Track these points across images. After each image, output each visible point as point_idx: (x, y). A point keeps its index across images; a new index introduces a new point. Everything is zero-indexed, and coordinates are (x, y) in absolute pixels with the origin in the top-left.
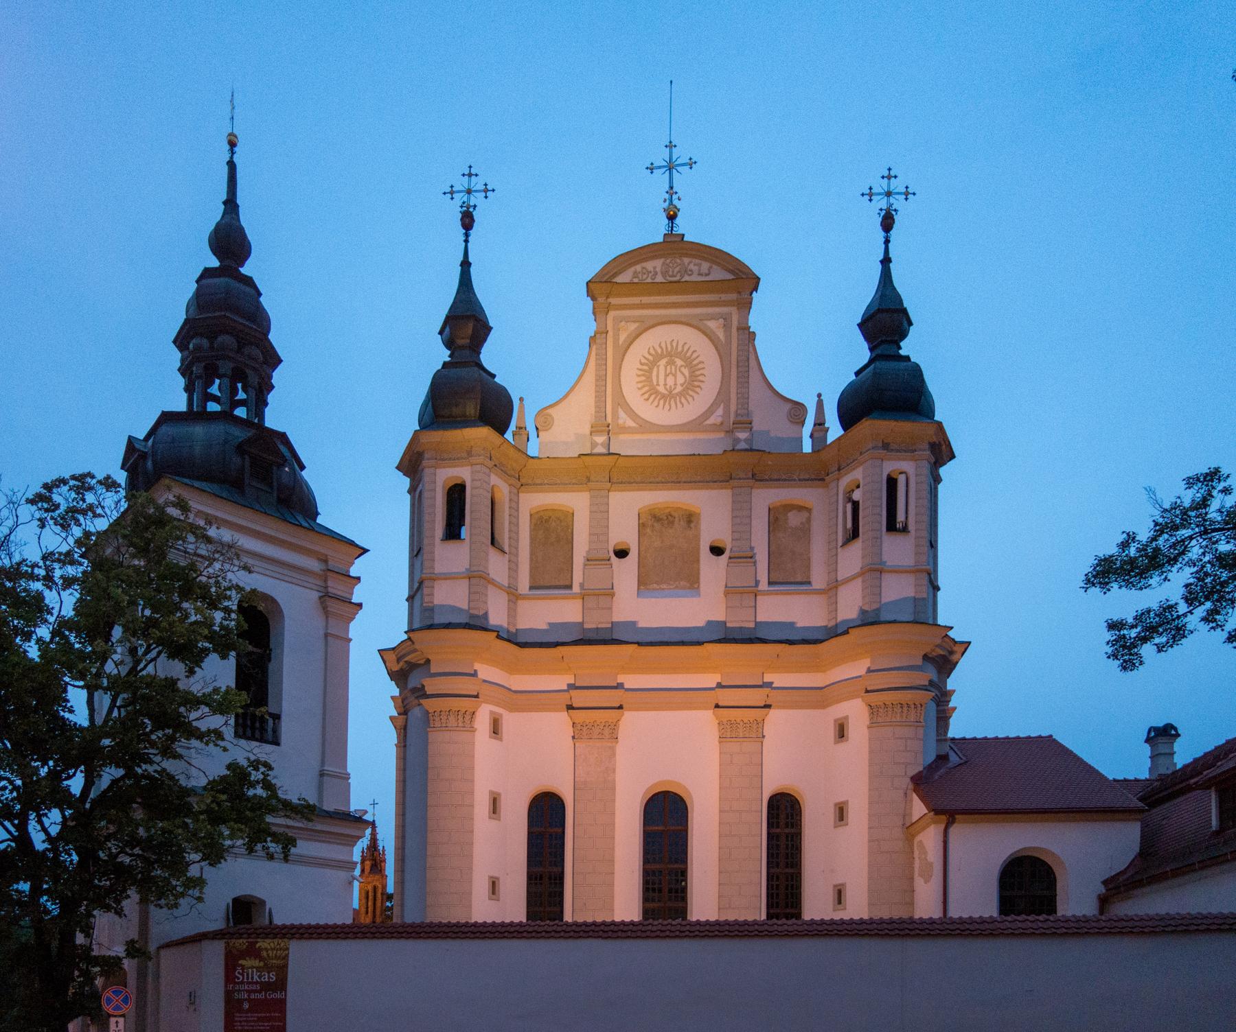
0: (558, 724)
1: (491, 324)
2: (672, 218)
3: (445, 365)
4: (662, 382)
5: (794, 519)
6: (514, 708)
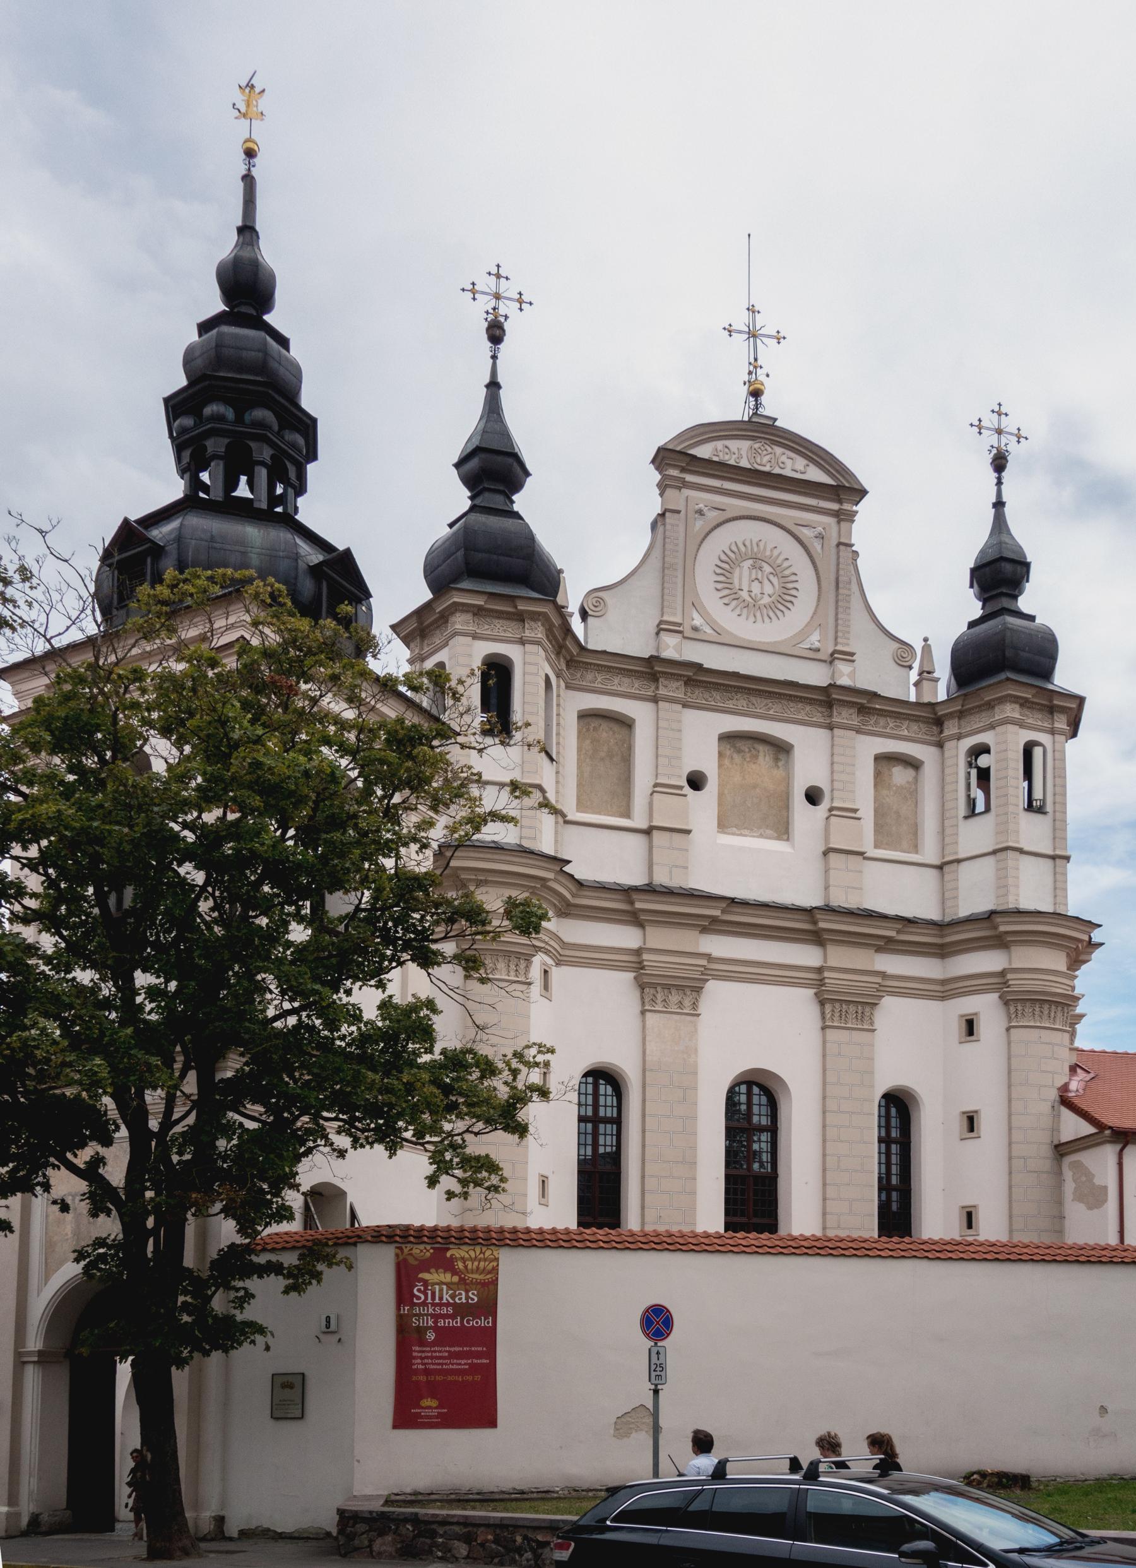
2: (756, 394)
5: (900, 775)
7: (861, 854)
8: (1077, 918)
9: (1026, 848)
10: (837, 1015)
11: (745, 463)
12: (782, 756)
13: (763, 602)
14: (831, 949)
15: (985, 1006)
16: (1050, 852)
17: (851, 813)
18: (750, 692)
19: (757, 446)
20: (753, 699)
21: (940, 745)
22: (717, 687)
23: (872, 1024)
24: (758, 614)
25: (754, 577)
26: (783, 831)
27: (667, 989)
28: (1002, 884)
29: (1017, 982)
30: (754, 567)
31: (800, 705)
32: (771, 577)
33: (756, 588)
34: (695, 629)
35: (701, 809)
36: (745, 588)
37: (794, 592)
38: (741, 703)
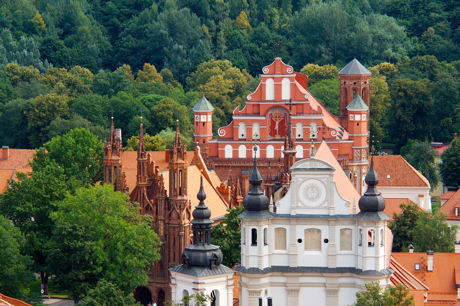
26: (320, 249)
33: (312, 194)
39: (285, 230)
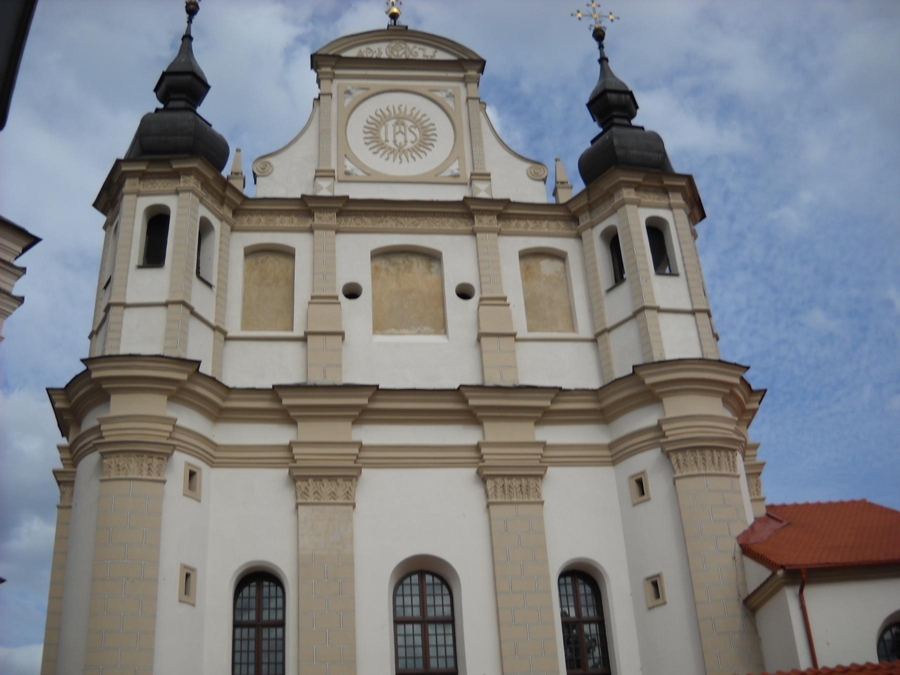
0: (272, 481)
1: (209, 82)
3: (157, 110)
4: (391, 137)
6: (212, 464)
7: (514, 335)
8: (720, 361)
9: (663, 305)
10: (500, 490)
11: (384, 56)
12: (435, 266)
13: (406, 147)
14: (487, 425)
15: (647, 461)
16: (688, 307)
17: (502, 301)
18: (396, 214)
19: (393, 44)
20: (401, 220)
21: (579, 237)
22: (367, 213)
23: (539, 496)
24: (403, 157)
25: (397, 129)
26: (442, 327)
27: (323, 480)
28: (645, 340)
29: (673, 432)
30: (397, 124)
31: (444, 219)
32: (413, 129)
33: (400, 138)
34: (347, 173)
35: (356, 317)
36: (391, 137)
37: (433, 137)
38: (390, 223)
39: (288, 253)
